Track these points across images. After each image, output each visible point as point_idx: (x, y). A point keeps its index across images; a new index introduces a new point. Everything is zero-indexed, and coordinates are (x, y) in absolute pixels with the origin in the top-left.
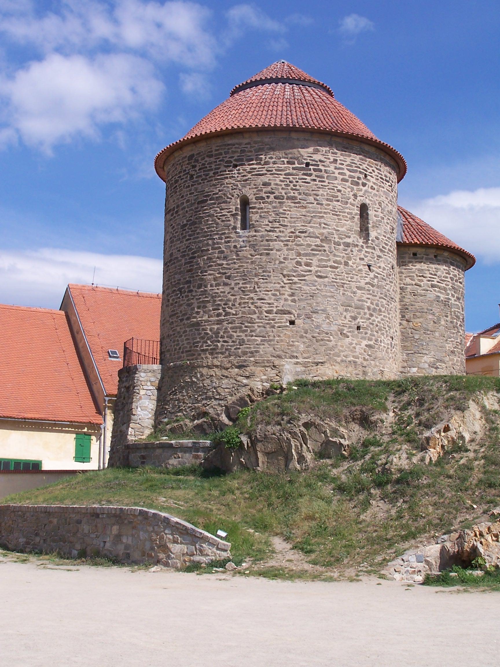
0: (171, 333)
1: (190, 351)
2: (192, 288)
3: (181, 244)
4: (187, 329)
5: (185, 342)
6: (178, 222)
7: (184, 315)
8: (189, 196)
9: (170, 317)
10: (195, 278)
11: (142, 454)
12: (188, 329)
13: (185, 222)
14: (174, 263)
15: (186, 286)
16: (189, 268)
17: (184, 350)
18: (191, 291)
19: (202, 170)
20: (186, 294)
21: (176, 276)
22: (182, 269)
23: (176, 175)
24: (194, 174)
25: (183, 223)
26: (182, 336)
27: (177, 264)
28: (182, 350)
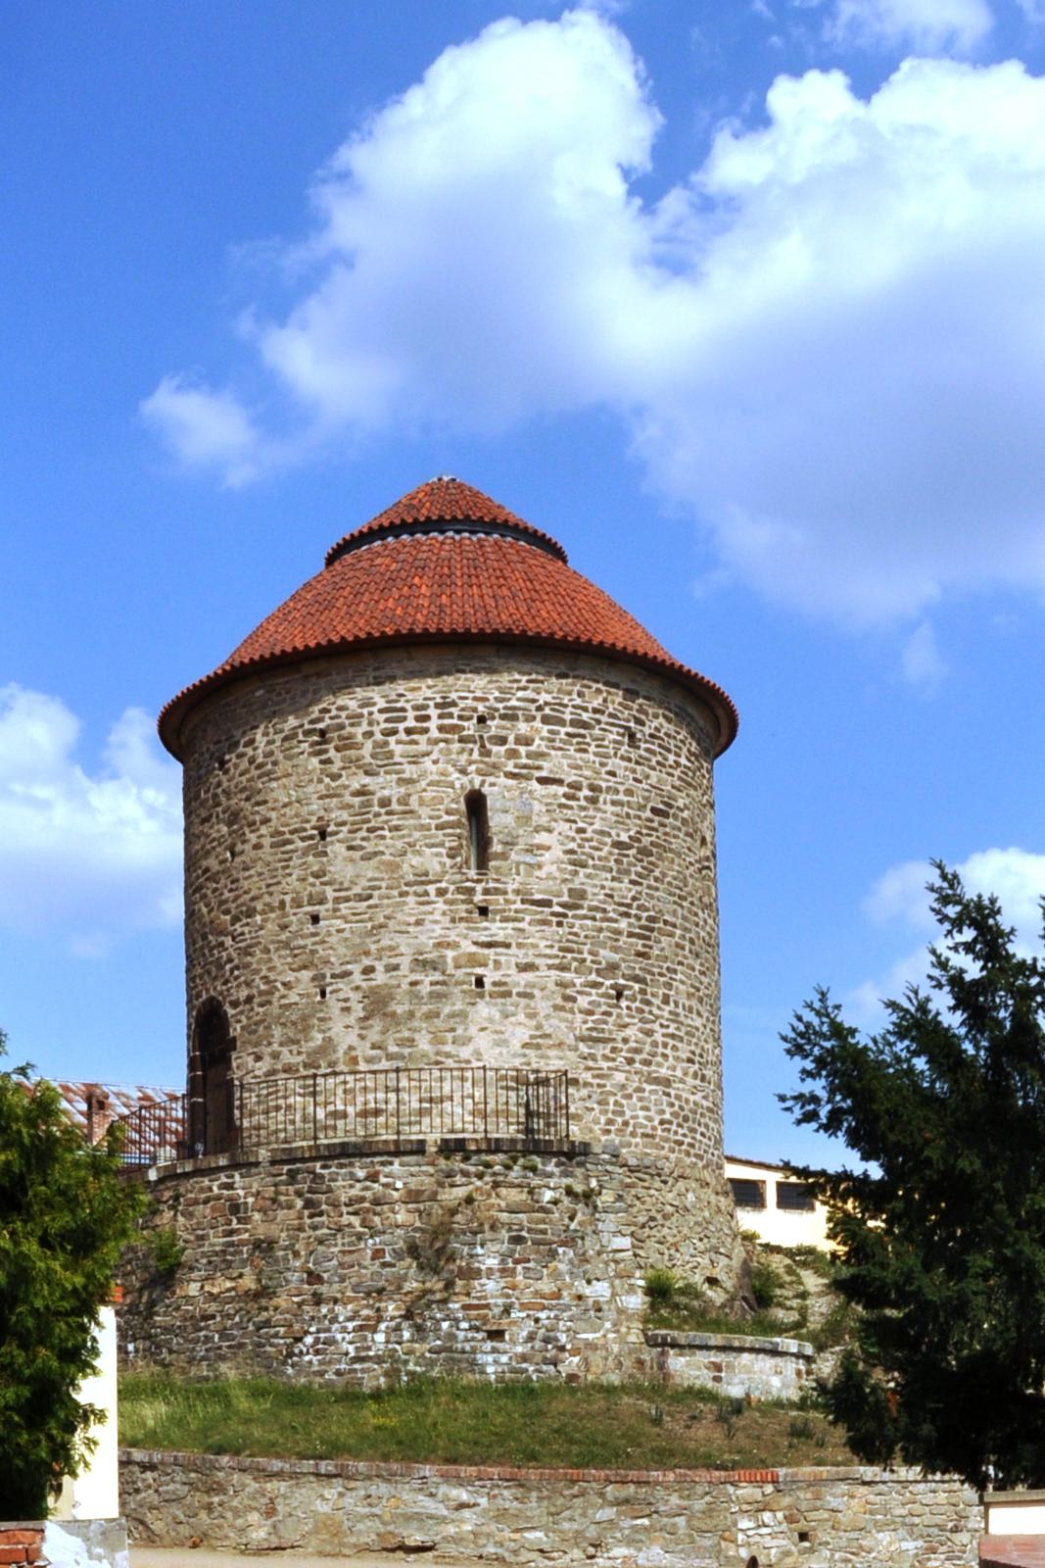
0: (587, 1076)
1: (653, 1136)
2: (649, 997)
3: (615, 884)
4: (645, 1085)
5: (641, 1113)
6: (596, 826)
7: (637, 1051)
8: (631, 782)
9: (582, 1039)
10: (657, 977)
11: (713, 1359)
12: (648, 1087)
13: (624, 837)
14: (594, 919)
15: (637, 987)
16: (640, 948)
17: (640, 1131)
18: (648, 1003)
19: (656, 741)
20: (637, 1004)
21: (602, 952)
22: (621, 943)
23: (585, 709)
24: (640, 740)
25: (618, 835)
26: (629, 1097)
27: (605, 925)
28: (630, 1128)
